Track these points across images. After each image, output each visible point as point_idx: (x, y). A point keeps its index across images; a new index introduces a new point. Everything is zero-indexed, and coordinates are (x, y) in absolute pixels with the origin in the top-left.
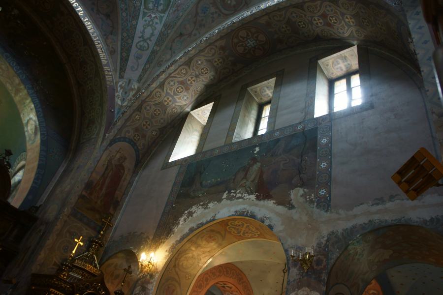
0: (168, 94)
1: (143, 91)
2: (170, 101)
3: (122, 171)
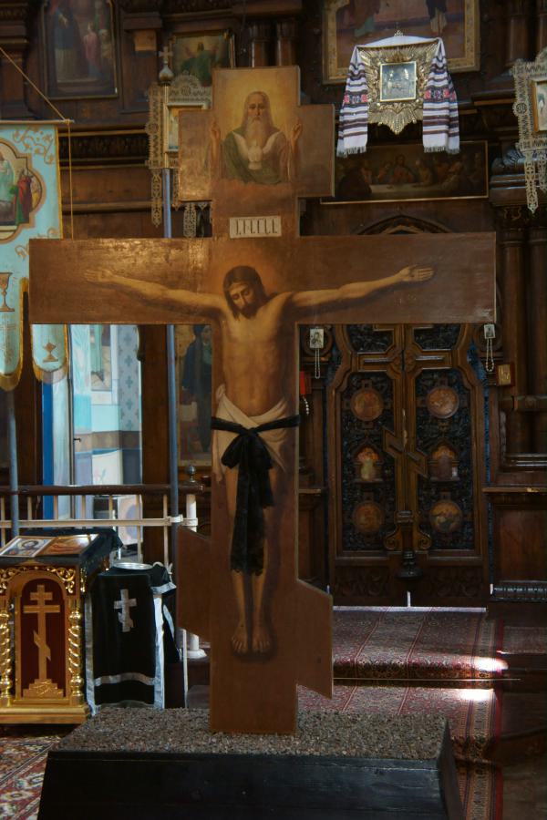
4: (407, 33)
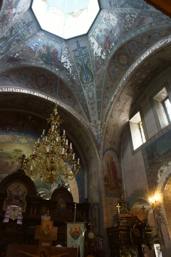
0: (115, 119)
1: (104, 123)
2: (118, 121)
3: (114, 164)
4: (16, 205)
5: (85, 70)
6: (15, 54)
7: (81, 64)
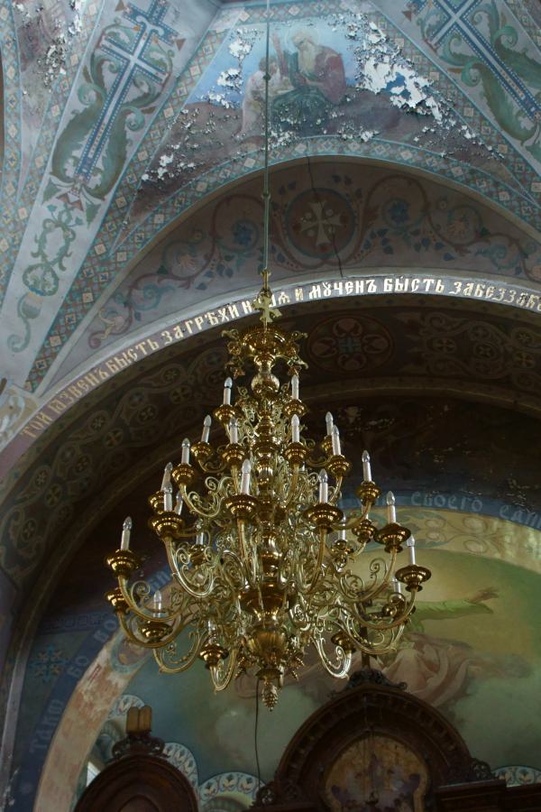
5: (499, 68)
6: (156, 165)
7: (470, 52)
